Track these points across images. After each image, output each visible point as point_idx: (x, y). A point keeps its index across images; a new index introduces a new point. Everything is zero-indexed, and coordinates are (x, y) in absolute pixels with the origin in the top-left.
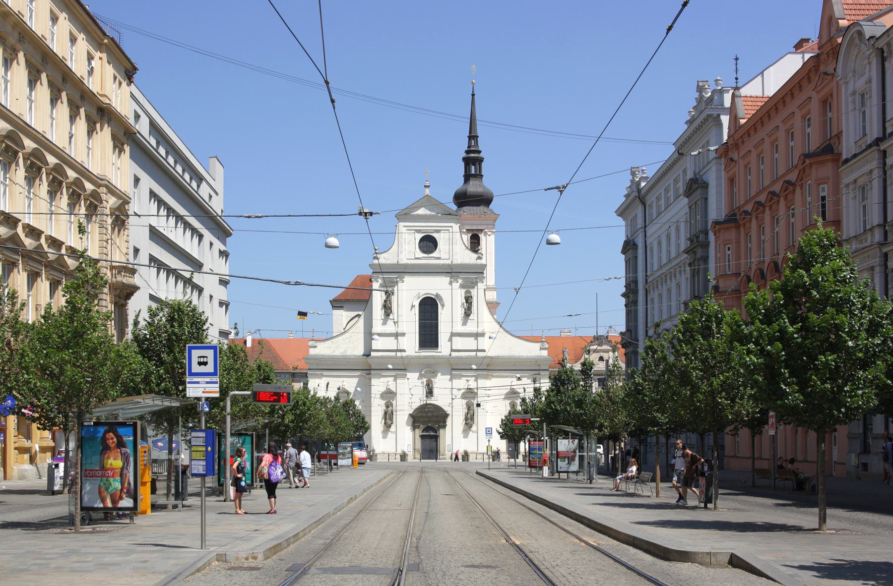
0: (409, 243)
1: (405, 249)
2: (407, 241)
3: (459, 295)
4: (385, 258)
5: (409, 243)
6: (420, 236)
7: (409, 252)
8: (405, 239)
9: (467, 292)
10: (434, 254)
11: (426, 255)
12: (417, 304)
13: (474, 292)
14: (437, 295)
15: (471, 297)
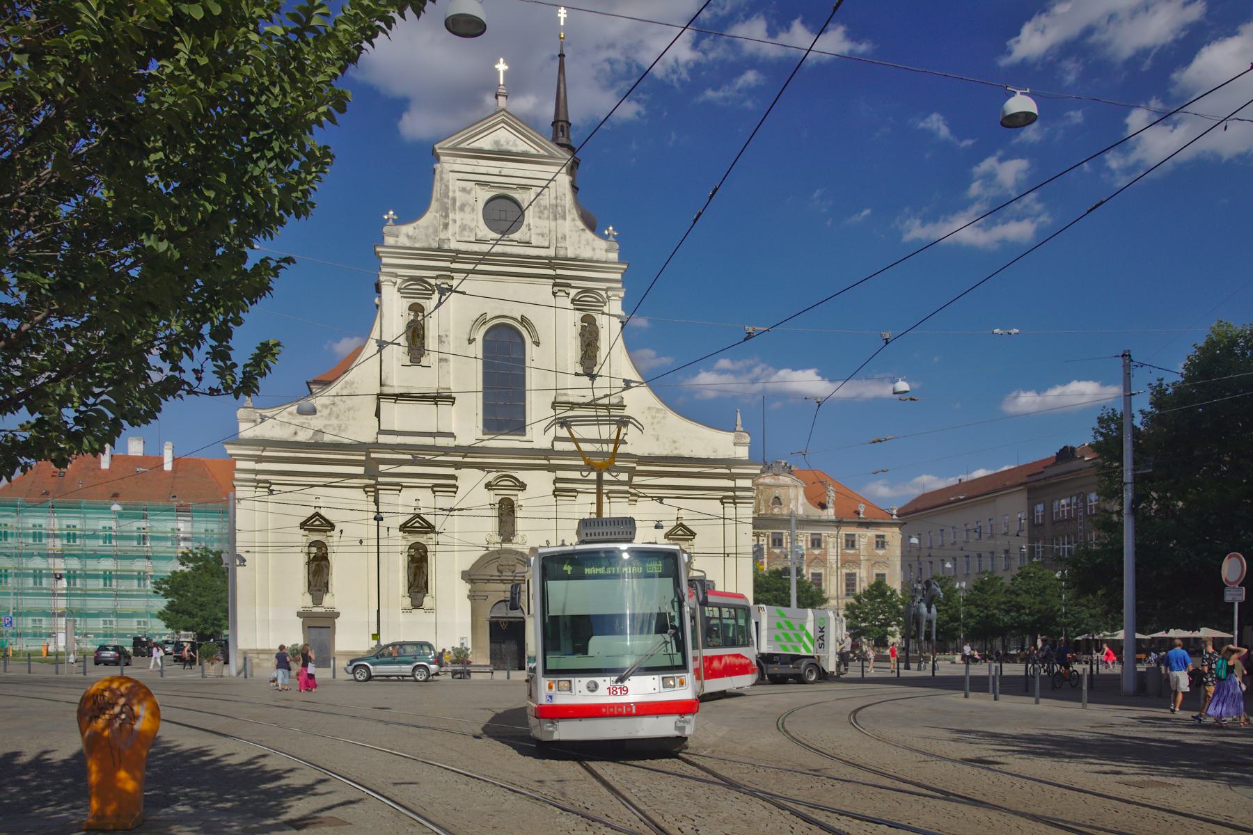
0: (462, 208)
1: (455, 221)
2: (458, 204)
3: (571, 320)
4: (408, 236)
5: (462, 208)
6: (485, 195)
7: (463, 228)
8: (454, 200)
12: (479, 336)
13: (601, 321)
14: (524, 320)
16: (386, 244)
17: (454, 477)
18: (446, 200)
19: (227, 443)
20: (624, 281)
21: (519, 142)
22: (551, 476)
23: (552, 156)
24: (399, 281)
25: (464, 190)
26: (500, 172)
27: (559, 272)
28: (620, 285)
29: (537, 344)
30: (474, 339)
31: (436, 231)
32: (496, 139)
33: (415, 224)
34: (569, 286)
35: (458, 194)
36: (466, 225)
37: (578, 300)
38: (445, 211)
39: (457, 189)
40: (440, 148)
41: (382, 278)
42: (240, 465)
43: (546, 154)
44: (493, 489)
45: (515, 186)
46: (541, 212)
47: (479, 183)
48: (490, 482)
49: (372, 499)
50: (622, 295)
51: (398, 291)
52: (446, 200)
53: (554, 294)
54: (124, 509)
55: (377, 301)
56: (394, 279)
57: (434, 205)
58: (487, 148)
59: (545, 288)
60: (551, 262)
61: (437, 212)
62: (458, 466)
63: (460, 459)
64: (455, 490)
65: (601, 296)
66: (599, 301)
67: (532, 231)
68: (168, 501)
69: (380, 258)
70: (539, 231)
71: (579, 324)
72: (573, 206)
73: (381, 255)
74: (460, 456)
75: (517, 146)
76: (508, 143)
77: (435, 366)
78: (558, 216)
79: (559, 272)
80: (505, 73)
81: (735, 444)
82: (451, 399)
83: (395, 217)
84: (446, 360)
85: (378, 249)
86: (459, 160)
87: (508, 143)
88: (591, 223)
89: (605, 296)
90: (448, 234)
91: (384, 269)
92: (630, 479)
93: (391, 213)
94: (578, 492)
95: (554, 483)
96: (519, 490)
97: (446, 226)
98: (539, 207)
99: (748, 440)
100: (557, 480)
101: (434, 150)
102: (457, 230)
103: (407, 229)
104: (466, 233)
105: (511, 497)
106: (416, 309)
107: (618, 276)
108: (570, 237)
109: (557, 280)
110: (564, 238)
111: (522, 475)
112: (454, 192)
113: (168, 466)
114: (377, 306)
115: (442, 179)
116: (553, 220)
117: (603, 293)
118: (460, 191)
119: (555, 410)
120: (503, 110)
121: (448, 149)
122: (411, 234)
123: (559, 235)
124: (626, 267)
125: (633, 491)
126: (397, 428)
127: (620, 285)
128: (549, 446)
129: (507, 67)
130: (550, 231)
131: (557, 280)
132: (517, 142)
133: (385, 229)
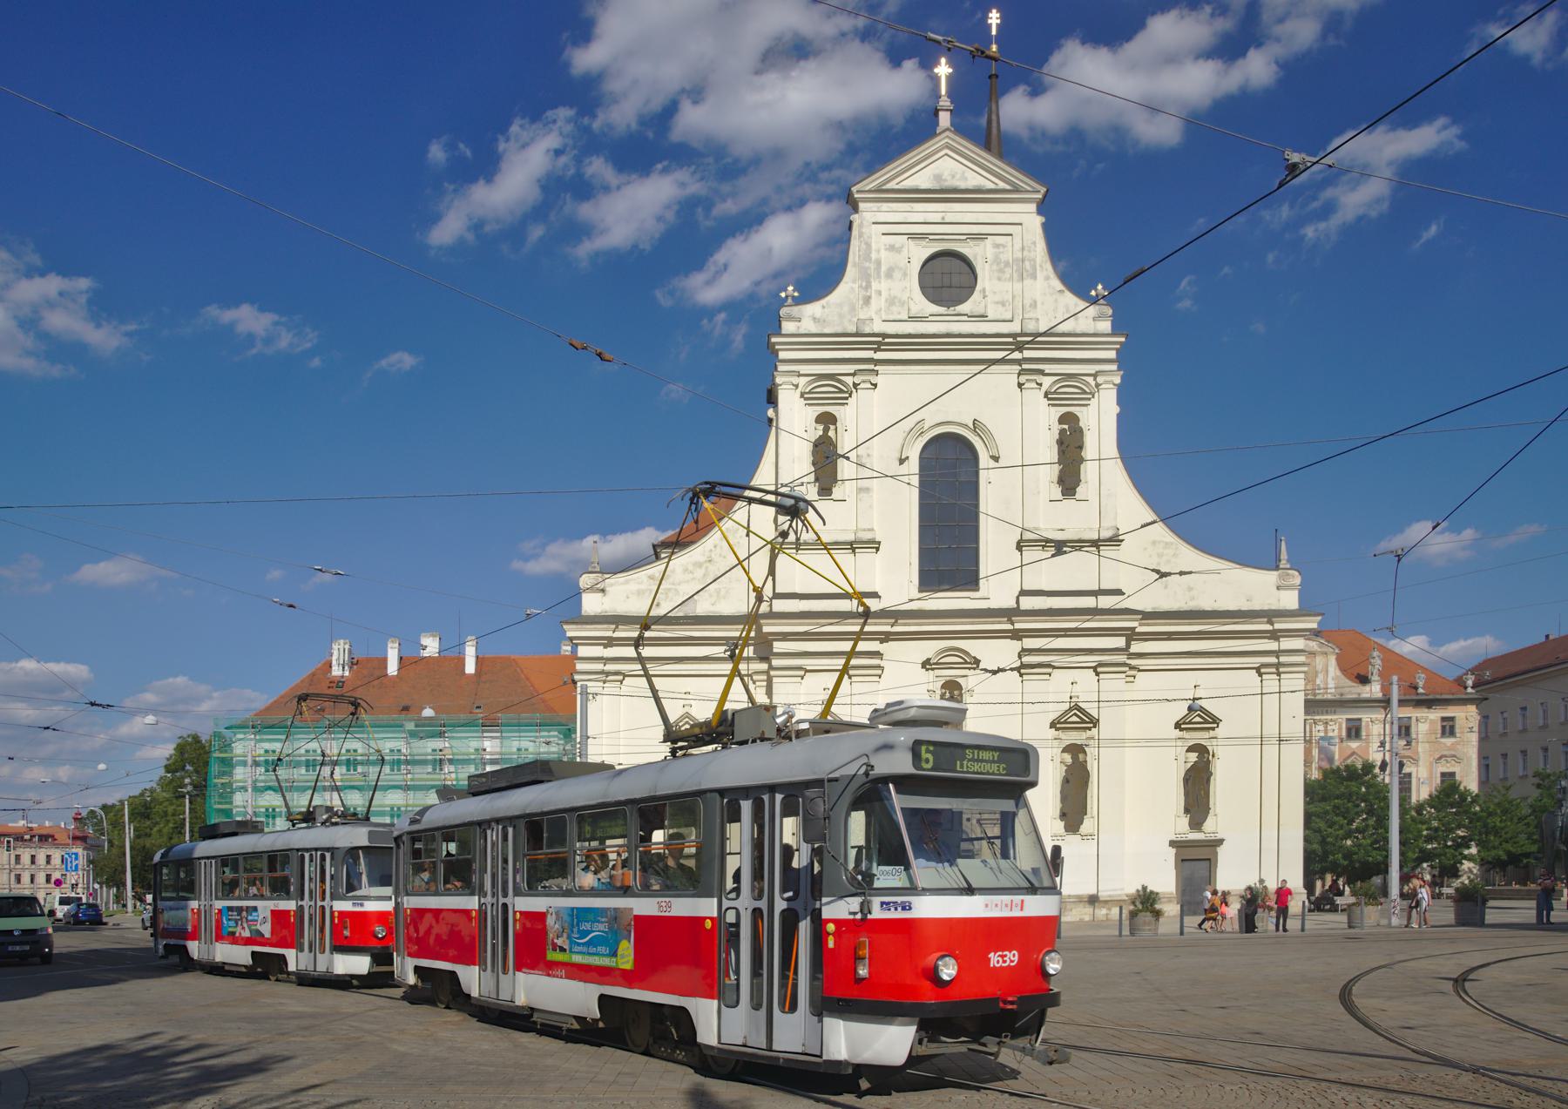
0: (889, 275)
1: (879, 293)
2: (884, 269)
3: (1043, 423)
5: (889, 275)
6: (923, 252)
7: (892, 301)
8: (878, 263)
9: (1069, 419)
10: (964, 308)
11: (942, 310)
12: (914, 453)
15: (1081, 431)
16: (783, 332)
17: (877, 654)
18: (867, 264)
19: (567, 623)
20: (1122, 360)
21: (969, 174)
22: (1016, 646)
23: (1016, 190)
24: (803, 381)
25: (891, 248)
26: (943, 218)
27: (1028, 354)
28: (1114, 367)
29: (996, 459)
30: (908, 457)
31: (853, 309)
32: (937, 172)
33: (823, 302)
34: (1042, 372)
35: (884, 254)
36: (895, 297)
37: (1055, 393)
38: (866, 278)
39: (883, 247)
40: (858, 192)
41: (778, 380)
42: (583, 651)
43: (1008, 187)
44: (933, 669)
45: (965, 237)
46: (1001, 271)
47: (913, 236)
48: (929, 659)
49: (764, 690)
50: (1118, 380)
51: (802, 395)
52: (867, 264)
53: (1020, 385)
54: (416, 726)
55: (771, 413)
56: (795, 380)
57: (851, 271)
58: (924, 186)
59: (1006, 378)
60: (1018, 342)
61: (854, 282)
62: (886, 637)
63: (887, 628)
64: (879, 672)
65: (1087, 384)
66: (1085, 393)
67: (989, 299)
68: (471, 713)
69: (778, 350)
70: (997, 298)
71: (1056, 428)
72: (1046, 258)
73: (777, 347)
74: (887, 624)
75: (965, 179)
76: (953, 177)
77: (851, 500)
78: (1025, 274)
79: (1028, 354)
80: (949, 78)
81: (1278, 588)
82: (875, 545)
83: (796, 294)
84: (867, 490)
85: (774, 340)
86: (885, 206)
87: (953, 177)
88: (1076, 281)
89: (1093, 383)
90: (871, 311)
91: (781, 368)
92: (1128, 645)
93: (790, 288)
94: (1054, 667)
95: (1020, 657)
96: (969, 669)
97: (867, 300)
98: (998, 264)
99: (1296, 579)
100: (1024, 650)
101: (850, 194)
102: (883, 304)
103: (813, 309)
104: (894, 309)
105: (959, 680)
106: (827, 420)
107: (1112, 355)
108: (1043, 303)
109: (1025, 366)
110: (1034, 305)
111: (973, 647)
112: (878, 251)
113: (470, 668)
114: (770, 420)
115: (861, 235)
116: (1018, 281)
117: (1090, 380)
118: (886, 249)
119: (1021, 551)
120: (947, 129)
121: (870, 191)
122: (818, 315)
123: (1027, 302)
124: (1123, 339)
125: (1133, 662)
126: (798, 590)
127: (1114, 367)
128: (1012, 604)
129: (951, 70)
130: (1013, 297)
131: (1025, 366)
132: (966, 175)
133: (783, 312)
